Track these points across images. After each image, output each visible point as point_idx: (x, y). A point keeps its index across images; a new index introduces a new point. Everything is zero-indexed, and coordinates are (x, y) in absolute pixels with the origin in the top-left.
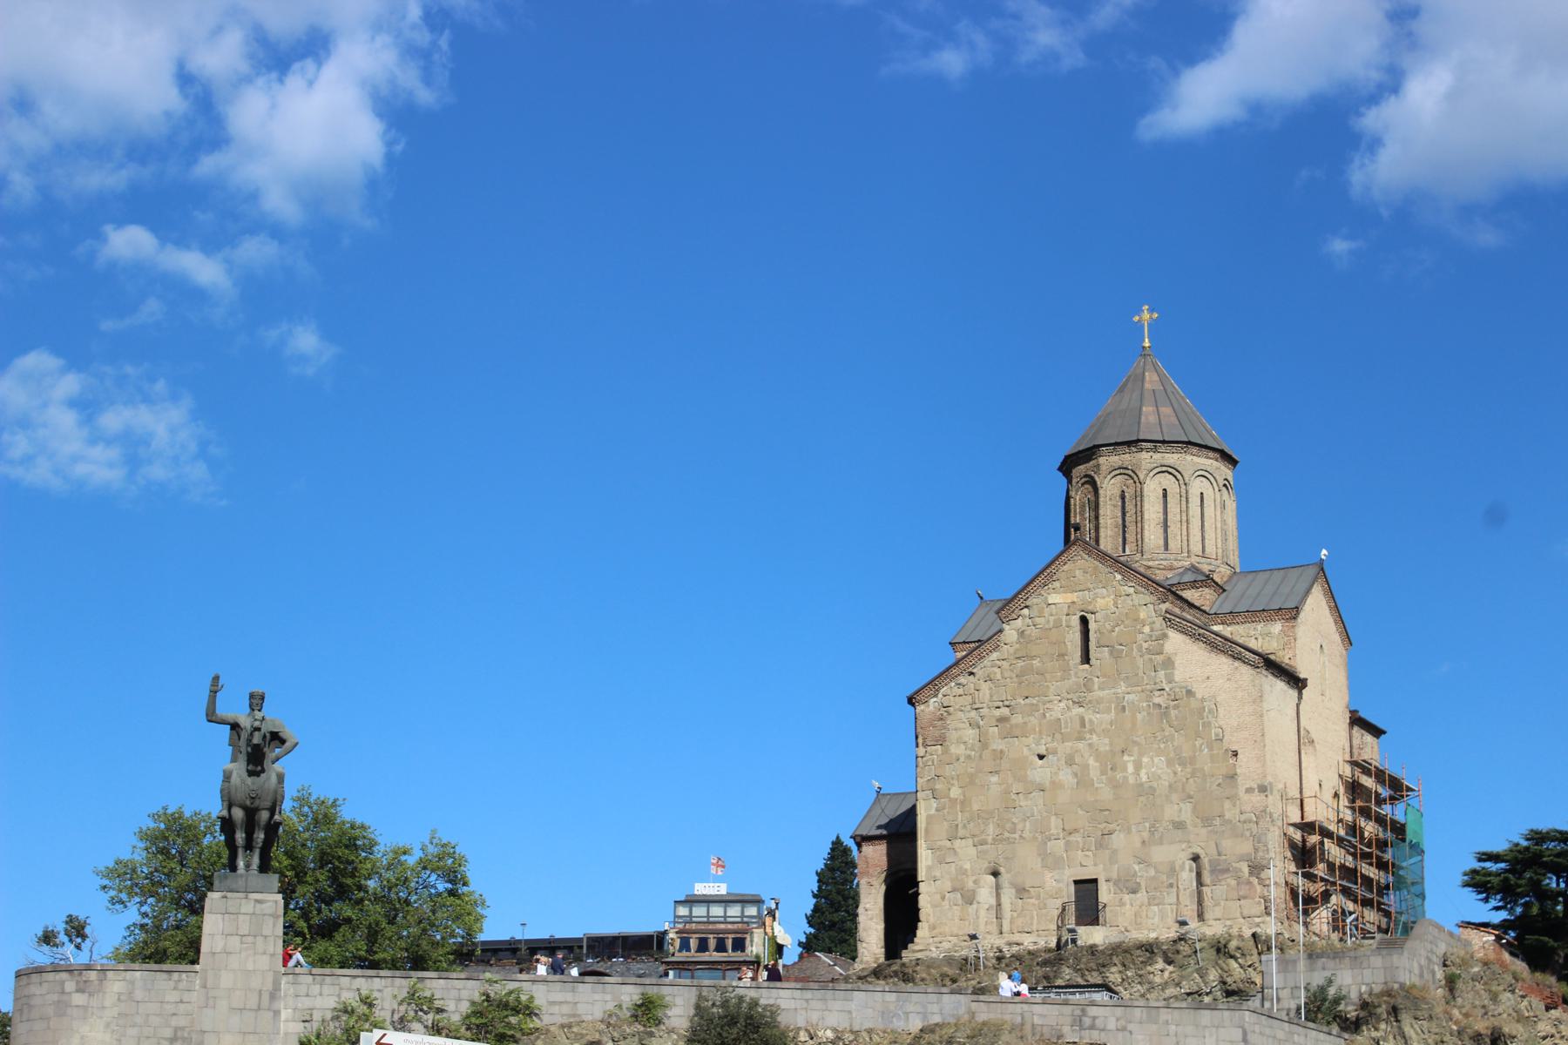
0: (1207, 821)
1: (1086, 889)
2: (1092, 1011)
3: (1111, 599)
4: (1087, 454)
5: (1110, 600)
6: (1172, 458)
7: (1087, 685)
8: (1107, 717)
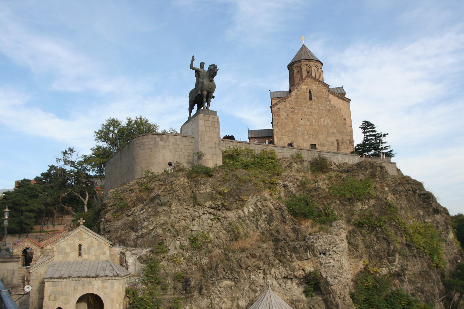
0: (339, 132)
3: (315, 87)
4: (300, 61)
5: (316, 88)
6: (316, 64)
7: (311, 105)
8: (316, 111)
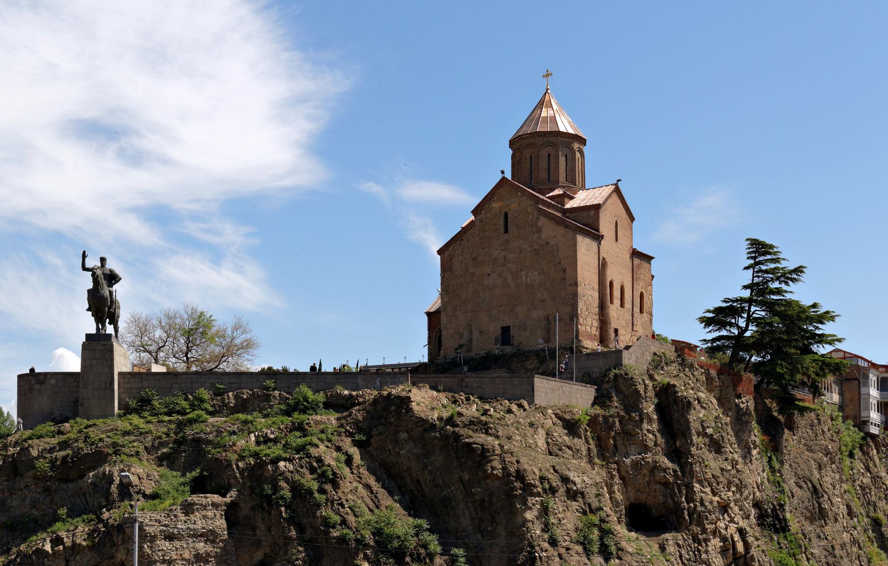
1: (506, 330)
2: (467, 380)
